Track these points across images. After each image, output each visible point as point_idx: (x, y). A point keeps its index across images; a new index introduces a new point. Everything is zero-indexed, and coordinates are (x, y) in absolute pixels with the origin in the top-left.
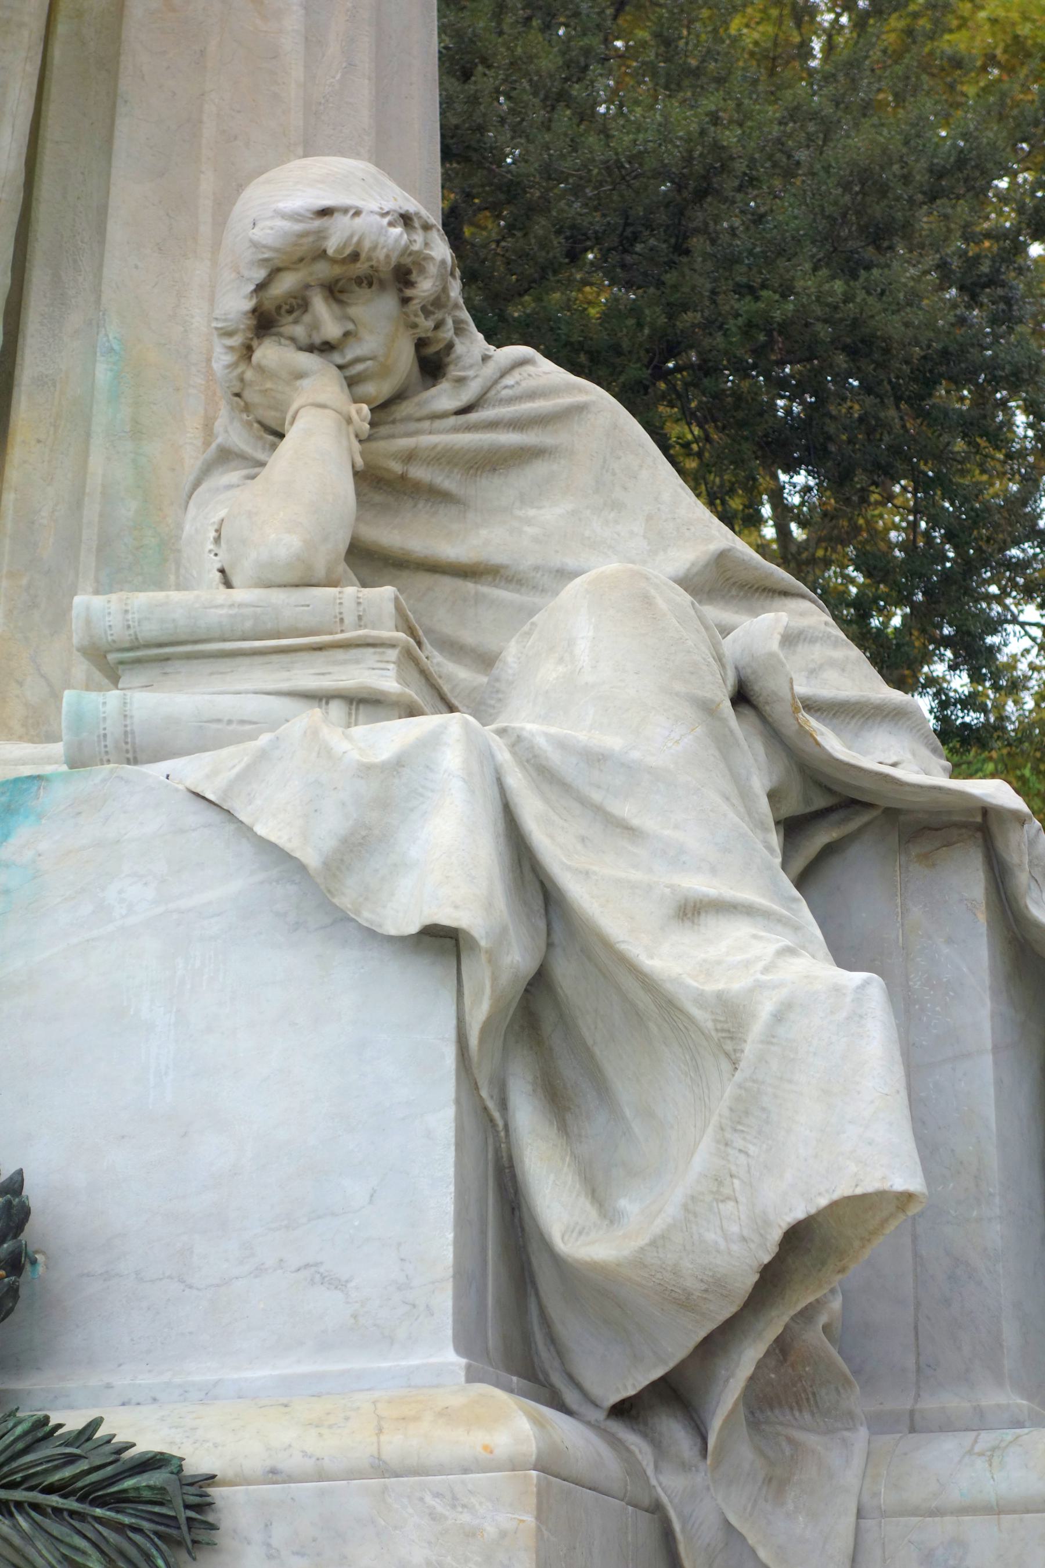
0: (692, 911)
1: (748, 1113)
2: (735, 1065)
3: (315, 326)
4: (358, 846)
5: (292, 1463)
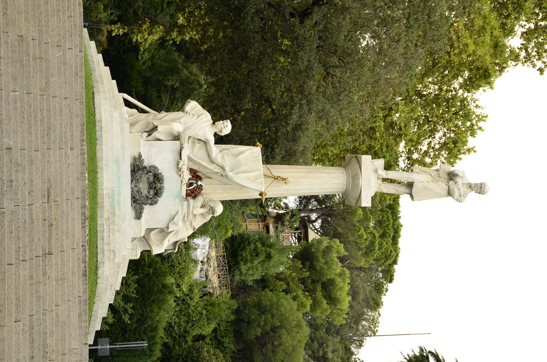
0: (169, 240)
1: (157, 245)
4: (174, 222)
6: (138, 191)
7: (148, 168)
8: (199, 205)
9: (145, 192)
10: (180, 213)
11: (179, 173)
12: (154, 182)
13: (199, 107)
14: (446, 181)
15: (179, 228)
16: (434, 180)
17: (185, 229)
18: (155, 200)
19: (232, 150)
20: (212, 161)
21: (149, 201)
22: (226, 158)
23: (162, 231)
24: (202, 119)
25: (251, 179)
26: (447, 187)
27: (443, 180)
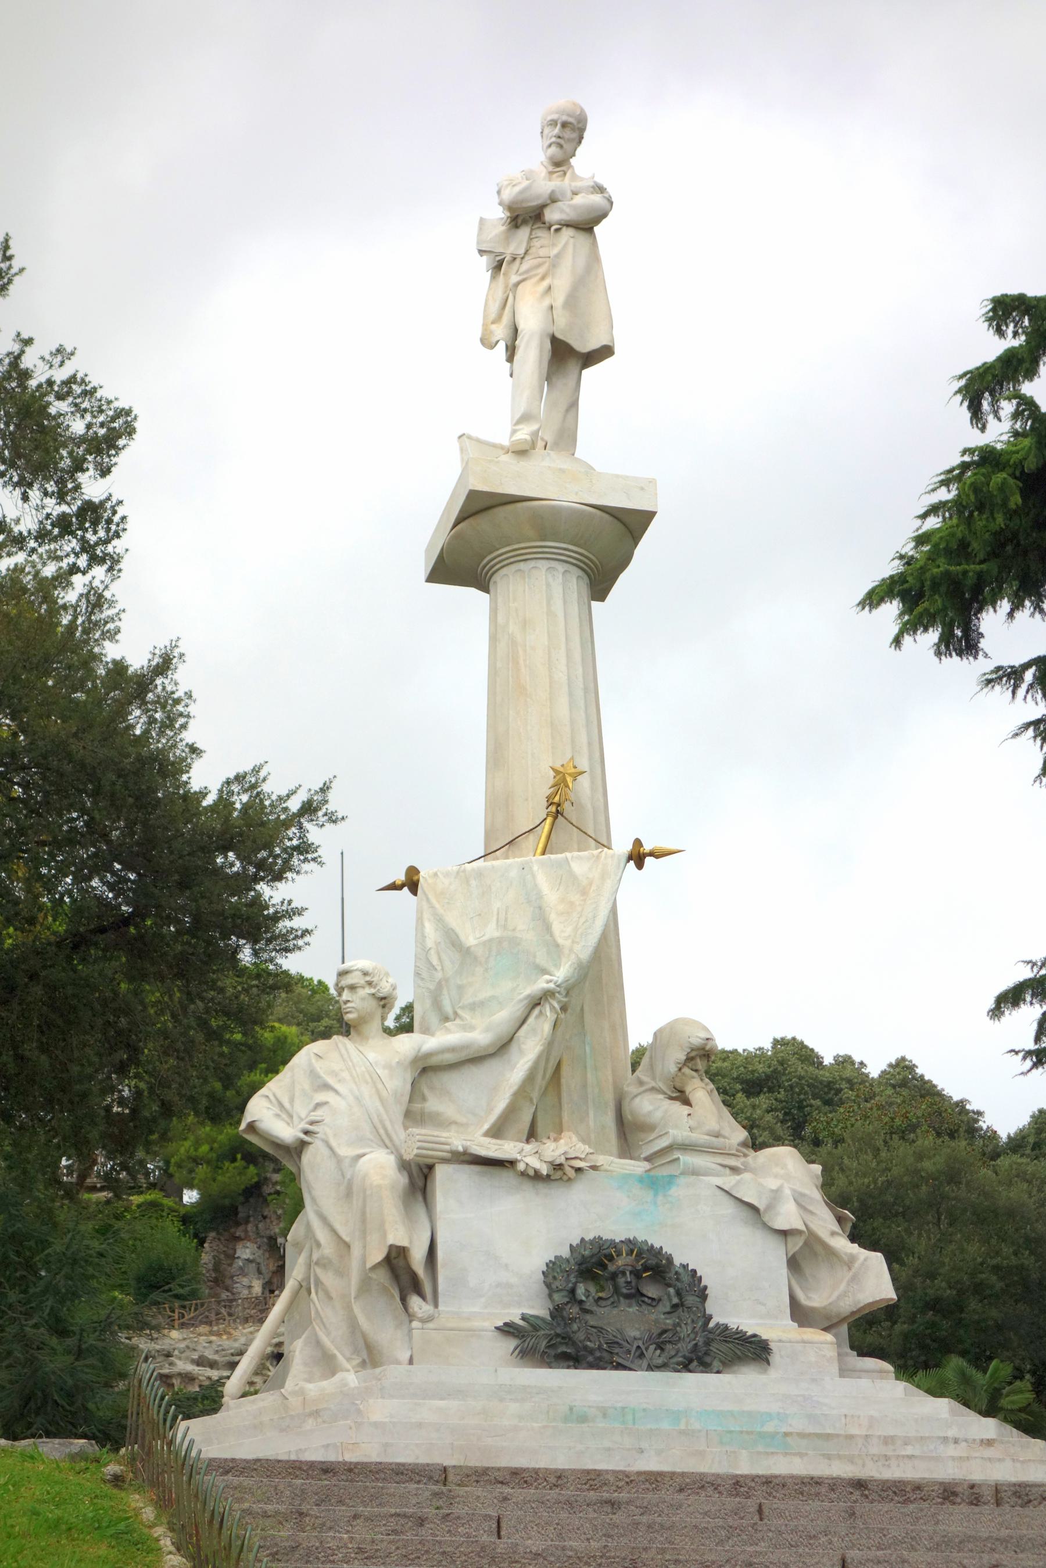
0: (833, 1234)
1: (854, 1279)
2: (850, 1269)
3: (696, 1065)
5: (784, 1339)
6: (660, 1347)
7: (559, 1298)
8: (686, 1109)
9: (659, 1317)
10: (728, 1181)
11: (571, 1173)
12: (614, 1276)
13: (276, 1086)
15: (787, 1192)
16: (541, 271)
17: (777, 1170)
18: (686, 1278)
20: (503, 1047)
21: (691, 1300)
23: (794, 1264)
24: (334, 1074)
25: (576, 898)
26: (567, 233)
27: (536, 243)
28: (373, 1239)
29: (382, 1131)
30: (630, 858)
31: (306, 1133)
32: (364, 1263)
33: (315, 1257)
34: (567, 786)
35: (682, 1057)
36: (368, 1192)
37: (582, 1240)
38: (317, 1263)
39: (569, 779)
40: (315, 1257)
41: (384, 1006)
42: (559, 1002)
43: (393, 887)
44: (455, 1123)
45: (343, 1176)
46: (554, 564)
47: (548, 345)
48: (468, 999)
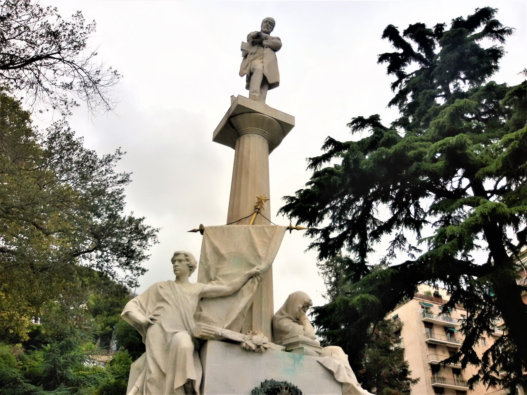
8: (301, 327)
10: (321, 359)
14: (262, 48)
16: (261, 57)
19: (210, 263)
20: (235, 293)
22: (229, 272)
24: (168, 295)
26: (268, 49)
27: (259, 50)
28: (179, 374)
29: (186, 322)
30: (288, 228)
31: (152, 319)
32: (173, 384)
33: (148, 377)
34: (262, 203)
35: (301, 306)
36: (179, 351)
37: (266, 380)
38: (148, 381)
39: (263, 201)
40: (148, 377)
41: (191, 270)
42: (260, 278)
43: (194, 231)
44: (213, 322)
45: (166, 340)
46: (260, 136)
47: (262, 76)
48: (221, 273)
